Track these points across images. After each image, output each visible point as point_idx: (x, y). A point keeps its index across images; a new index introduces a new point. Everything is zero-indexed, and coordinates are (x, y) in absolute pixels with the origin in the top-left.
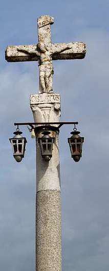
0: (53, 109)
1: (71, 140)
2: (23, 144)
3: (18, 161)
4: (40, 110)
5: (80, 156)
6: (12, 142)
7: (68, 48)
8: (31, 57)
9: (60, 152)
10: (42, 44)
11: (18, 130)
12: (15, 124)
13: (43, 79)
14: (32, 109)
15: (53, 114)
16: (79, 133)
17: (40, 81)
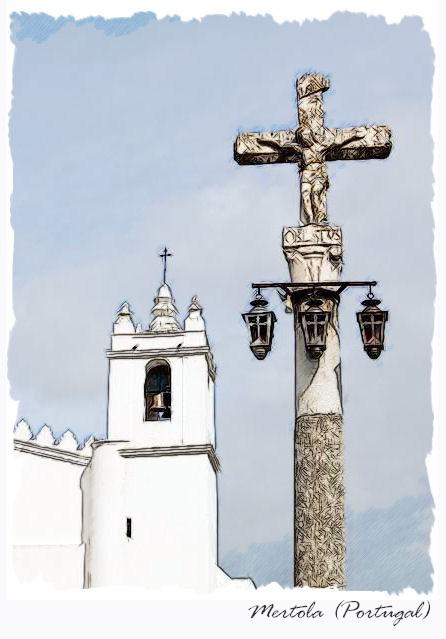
0: (327, 256)
1: (363, 317)
2: (269, 322)
3: (261, 357)
4: (301, 258)
5: (381, 348)
6: (247, 320)
7: (356, 138)
8: (284, 155)
9: (344, 339)
10: (307, 131)
11: (259, 297)
12: (254, 286)
13: (308, 197)
14: (286, 255)
15: (327, 265)
16: (379, 302)
17: (302, 201)
